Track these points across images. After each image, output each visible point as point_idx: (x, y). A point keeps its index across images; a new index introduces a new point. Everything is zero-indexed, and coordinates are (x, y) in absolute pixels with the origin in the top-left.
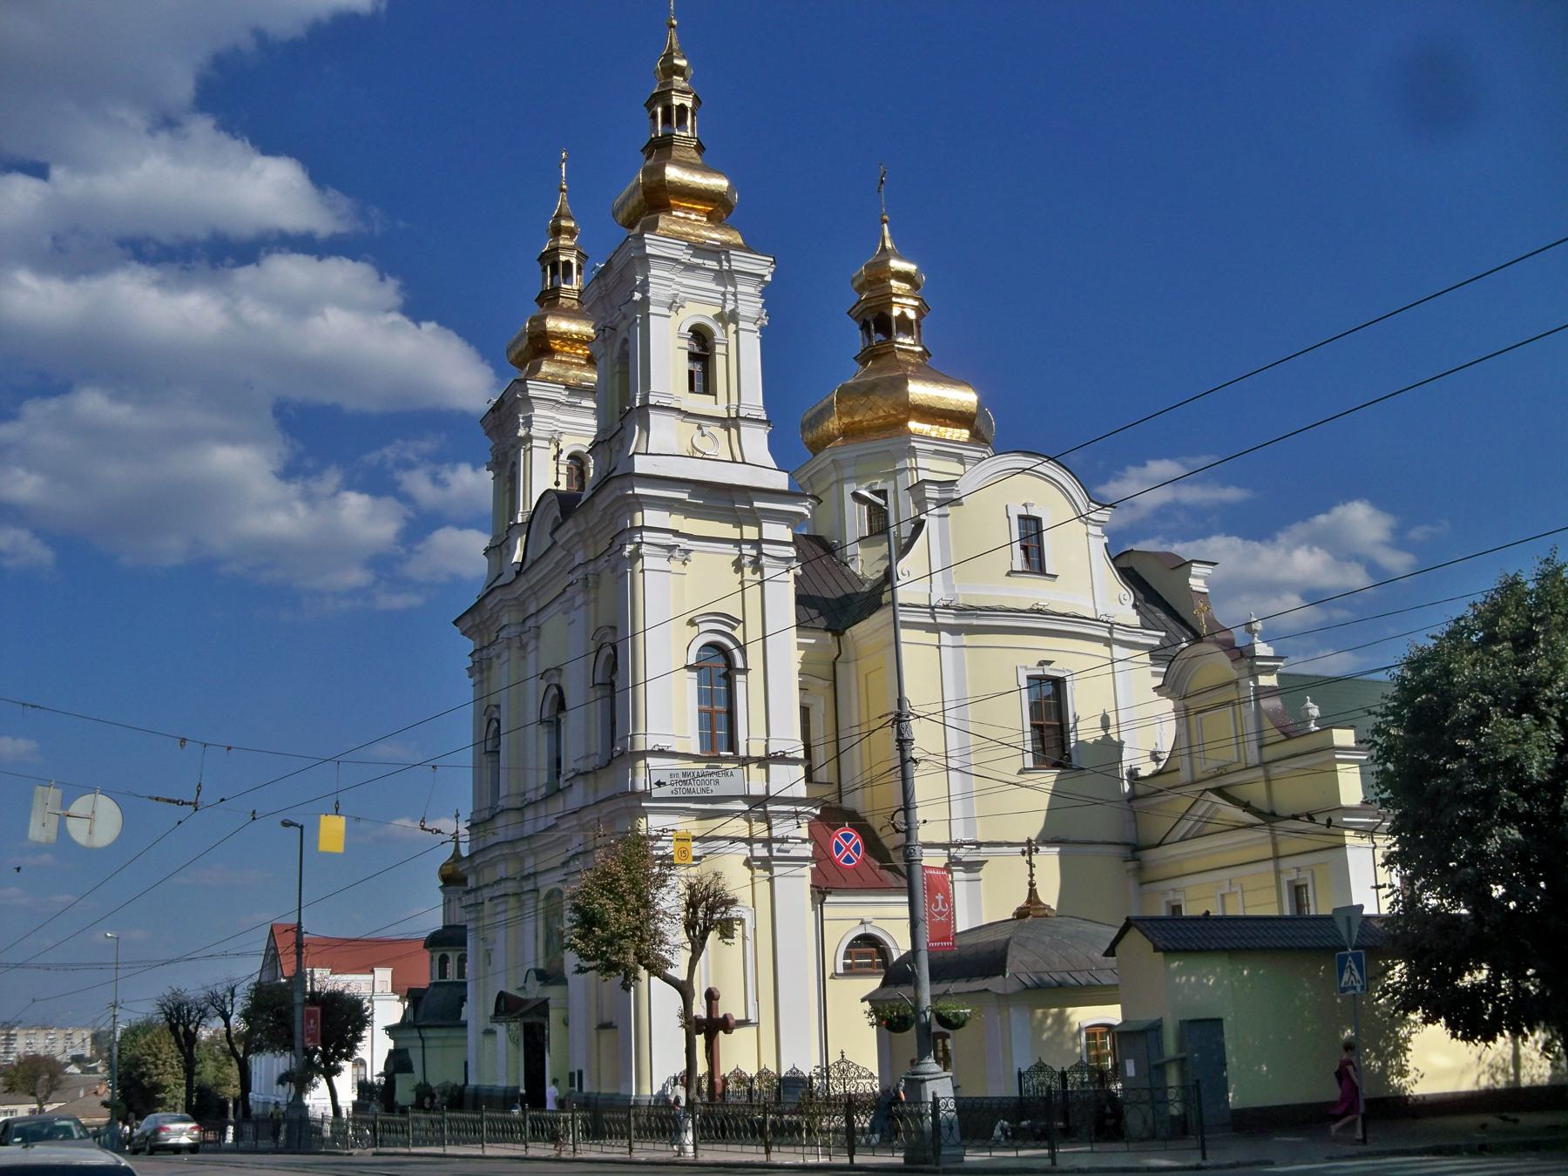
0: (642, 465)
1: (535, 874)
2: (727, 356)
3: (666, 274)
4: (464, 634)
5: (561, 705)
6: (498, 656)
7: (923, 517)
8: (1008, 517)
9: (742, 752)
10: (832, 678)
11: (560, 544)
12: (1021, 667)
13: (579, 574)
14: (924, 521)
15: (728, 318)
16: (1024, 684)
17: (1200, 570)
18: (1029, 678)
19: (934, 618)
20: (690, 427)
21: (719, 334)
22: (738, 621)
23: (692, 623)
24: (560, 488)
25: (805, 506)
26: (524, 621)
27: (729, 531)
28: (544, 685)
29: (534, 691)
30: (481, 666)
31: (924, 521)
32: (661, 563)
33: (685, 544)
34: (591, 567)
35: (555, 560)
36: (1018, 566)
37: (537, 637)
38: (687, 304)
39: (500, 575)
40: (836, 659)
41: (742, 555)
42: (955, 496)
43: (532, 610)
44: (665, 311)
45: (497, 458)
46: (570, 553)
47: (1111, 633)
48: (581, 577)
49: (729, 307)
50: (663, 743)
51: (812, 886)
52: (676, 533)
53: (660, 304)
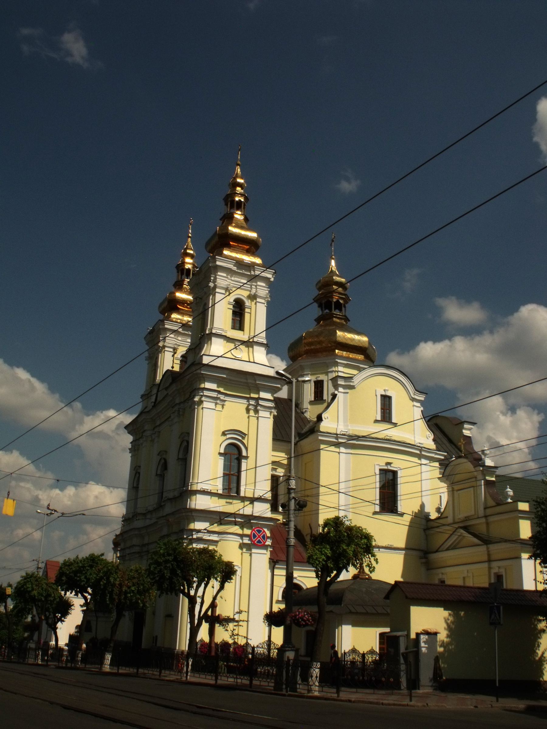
0: (206, 360)
1: (148, 544)
2: (250, 313)
5: (165, 467)
6: (142, 444)
7: (336, 392)
8: (376, 395)
9: (242, 494)
12: (377, 465)
13: (176, 408)
14: (337, 394)
15: (253, 297)
16: (378, 472)
18: (380, 470)
21: (248, 303)
22: (245, 434)
23: (224, 434)
24: (174, 369)
26: (154, 429)
31: (337, 394)
32: (212, 405)
33: (222, 397)
36: (379, 418)
41: (249, 405)
42: (352, 384)
43: (158, 423)
45: (150, 354)
47: (421, 452)
48: (177, 409)
49: (254, 291)
51: (269, 559)
52: (219, 392)
53: (222, 288)
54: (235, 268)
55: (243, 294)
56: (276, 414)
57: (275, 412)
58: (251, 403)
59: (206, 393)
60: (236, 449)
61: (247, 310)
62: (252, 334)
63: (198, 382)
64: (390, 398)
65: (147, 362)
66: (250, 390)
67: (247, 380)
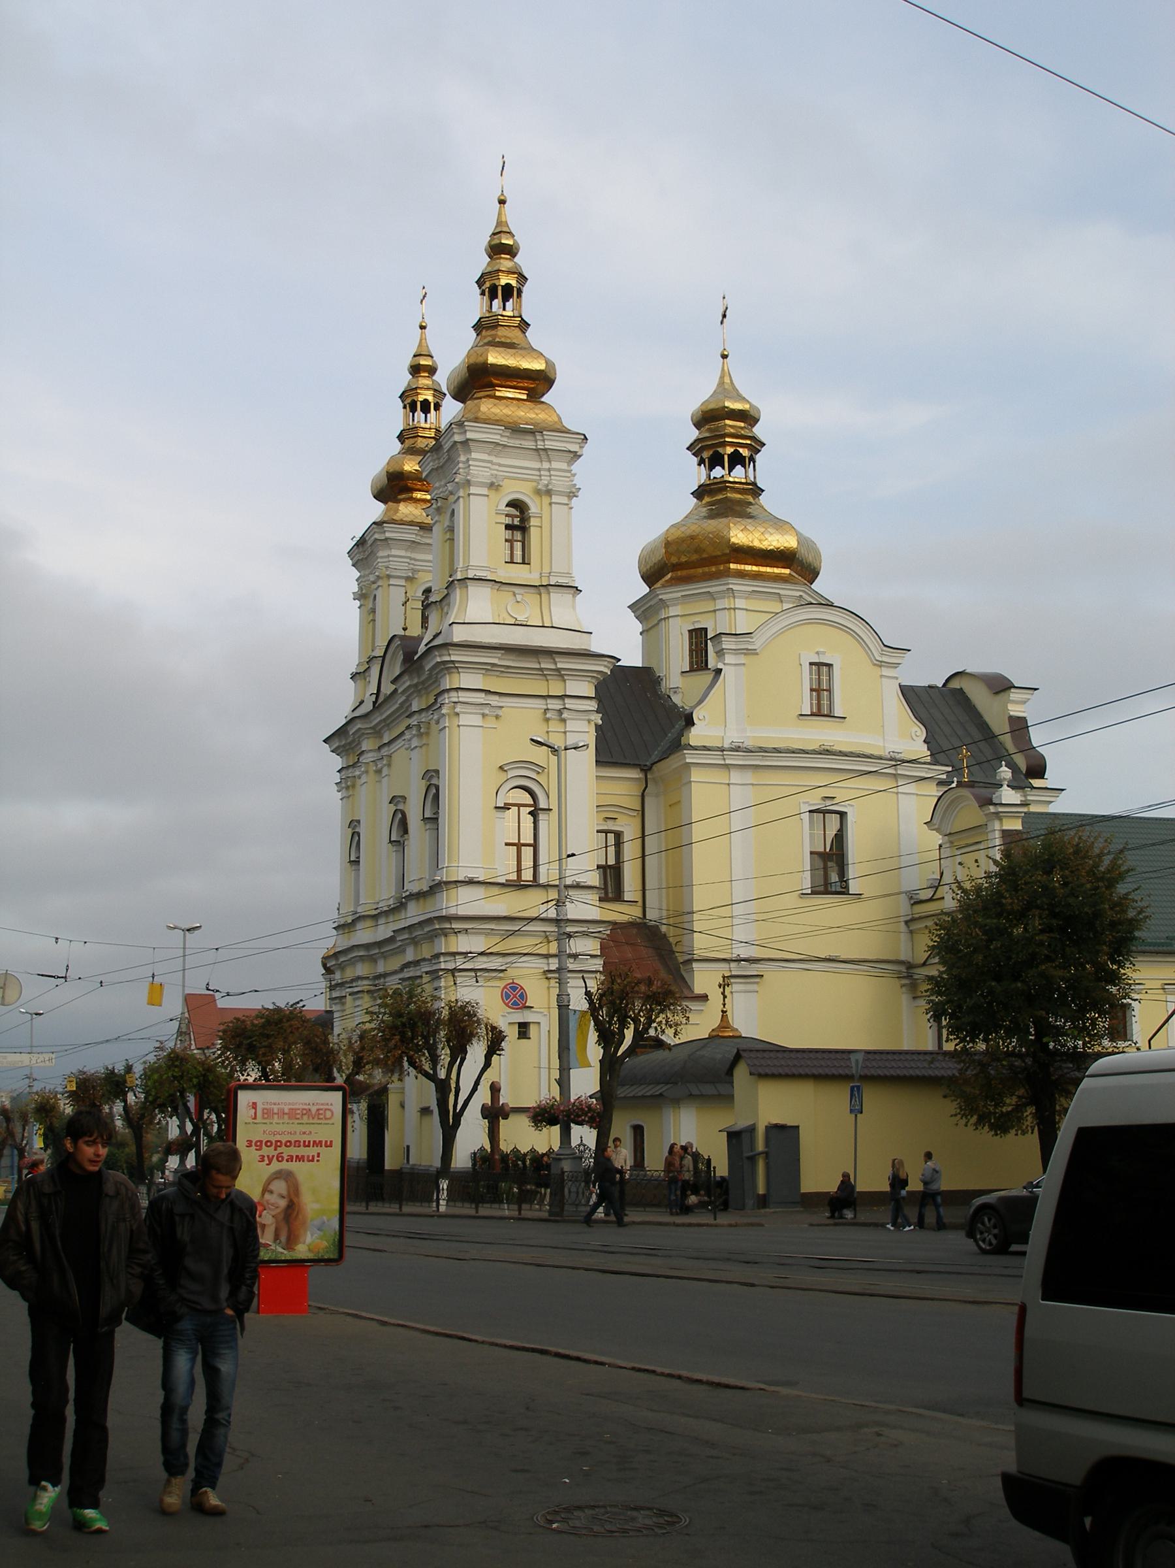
0: (459, 635)
3: (485, 457)
4: (332, 751)
6: (359, 777)
10: (639, 808)
11: (399, 691)
12: (804, 803)
13: (414, 721)
14: (721, 670)
17: (1020, 696)
19: (724, 759)
20: (506, 595)
21: (533, 509)
24: (408, 633)
25: (605, 666)
27: (539, 688)
28: (393, 808)
29: (387, 811)
30: (347, 784)
31: (721, 670)
32: (477, 720)
33: (494, 700)
34: (424, 717)
35: (399, 702)
37: (389, 765)
38: (506, 483)
39: (362, 702)
40: (644, 791)
43: (386, 740)
44: (485, 491)
46: (407, 702)
48: (415, 723)
50: (471, 875)
54: (504, 441)
55: (522, 491)
56: (600, 722)
57: (598, 719)
58: (550, 707)
59: (464, 697)
60: (528, 795)
61: (533, 522)
62: (546, 570)
63: (447, 676)
64: (829, 666)
65: (358, 603)
66: (547, 680)
67: (540, 663)
